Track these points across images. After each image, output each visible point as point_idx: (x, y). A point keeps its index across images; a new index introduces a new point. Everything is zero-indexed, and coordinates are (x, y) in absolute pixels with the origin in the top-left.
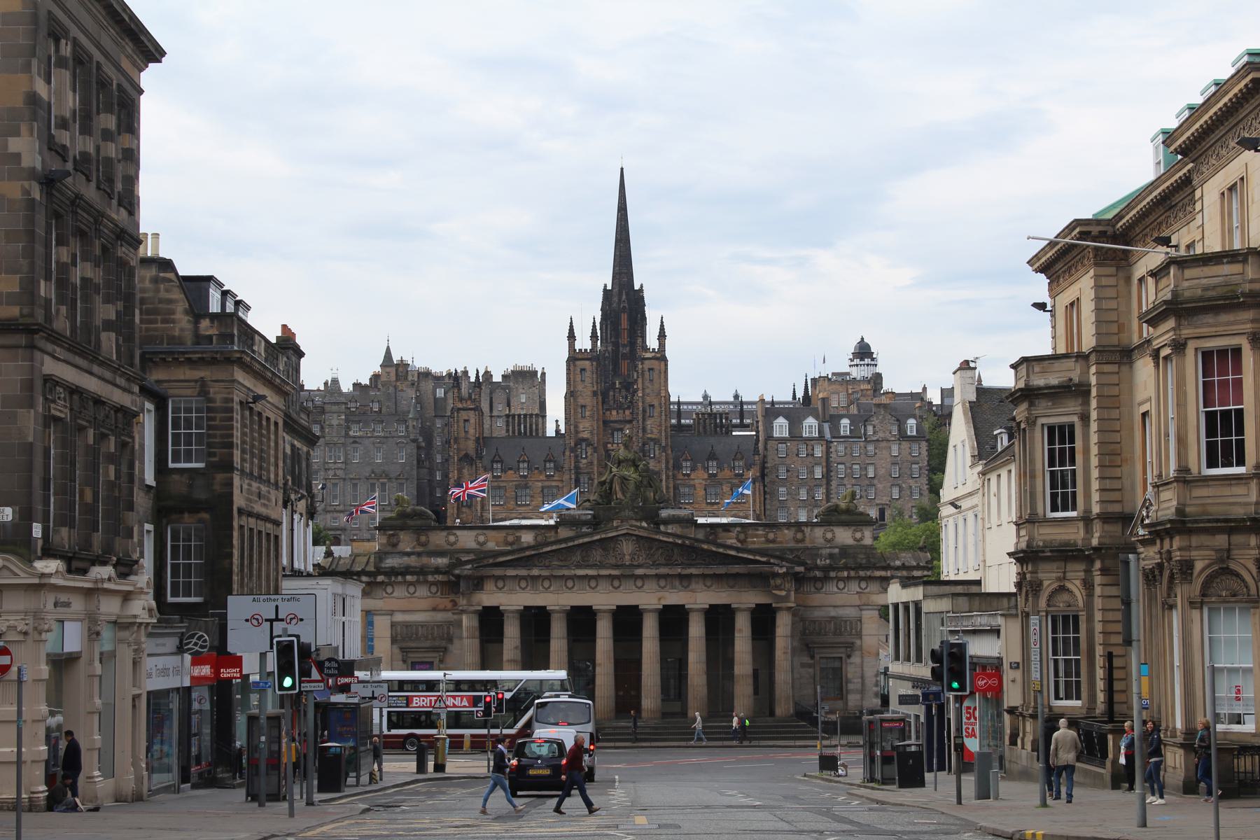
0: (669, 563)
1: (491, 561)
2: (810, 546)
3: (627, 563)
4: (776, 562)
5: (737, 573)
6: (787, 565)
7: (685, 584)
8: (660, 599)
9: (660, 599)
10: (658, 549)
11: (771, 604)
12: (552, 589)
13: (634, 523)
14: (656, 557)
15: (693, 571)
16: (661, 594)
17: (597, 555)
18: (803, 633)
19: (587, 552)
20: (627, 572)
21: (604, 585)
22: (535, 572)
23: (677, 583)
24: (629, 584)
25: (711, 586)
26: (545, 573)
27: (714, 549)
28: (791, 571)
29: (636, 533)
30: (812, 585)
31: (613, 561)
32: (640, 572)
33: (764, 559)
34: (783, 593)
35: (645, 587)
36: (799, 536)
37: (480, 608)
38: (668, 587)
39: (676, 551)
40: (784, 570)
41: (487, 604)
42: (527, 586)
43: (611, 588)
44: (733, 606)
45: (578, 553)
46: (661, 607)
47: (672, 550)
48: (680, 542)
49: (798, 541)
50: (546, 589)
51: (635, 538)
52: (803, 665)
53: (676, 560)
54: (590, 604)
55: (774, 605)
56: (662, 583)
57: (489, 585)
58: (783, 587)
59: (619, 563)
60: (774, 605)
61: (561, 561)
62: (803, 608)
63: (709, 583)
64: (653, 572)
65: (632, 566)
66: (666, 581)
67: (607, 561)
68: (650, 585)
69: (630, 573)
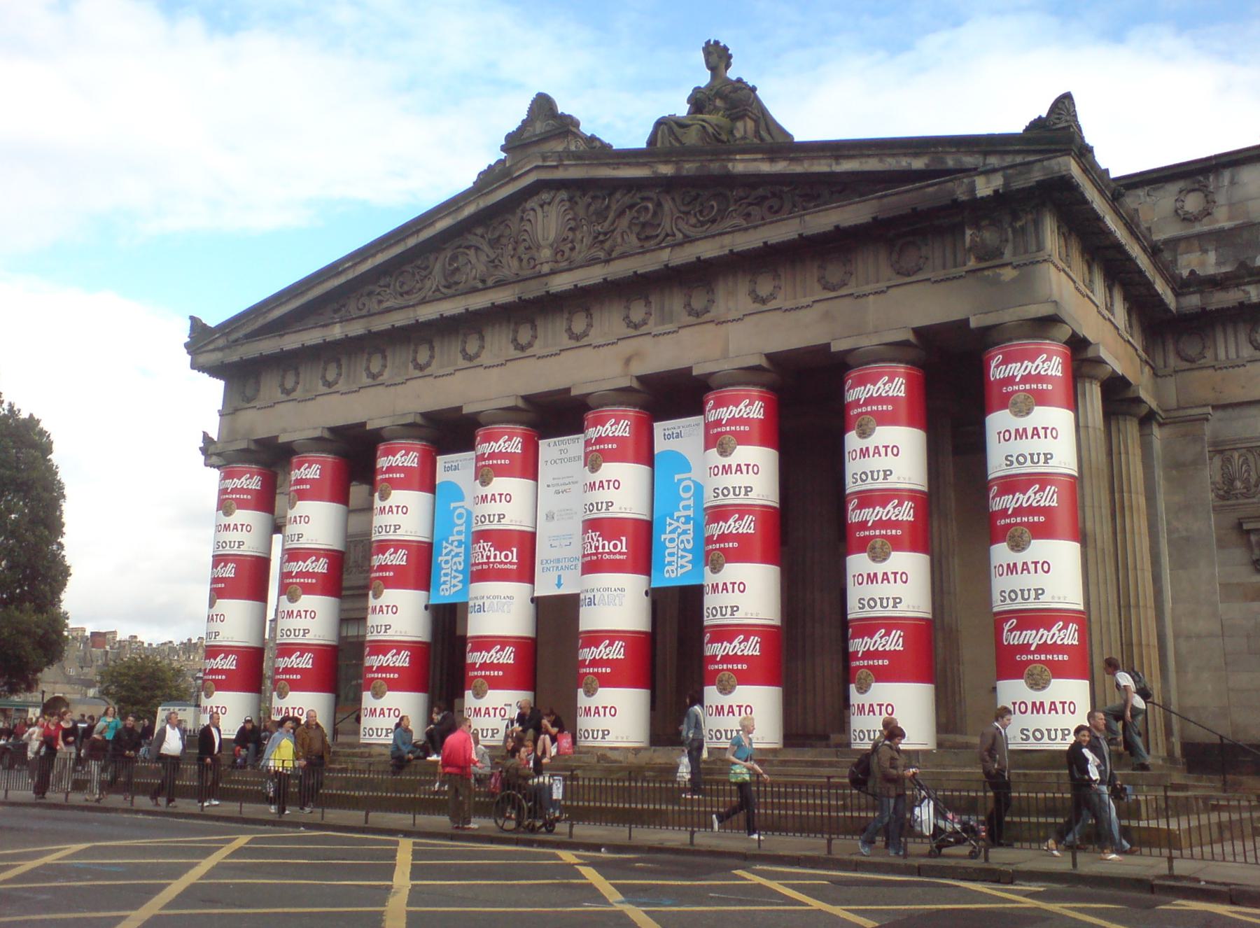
0: (648, 236)
1: (261, 322)
2: (1227, 225)
3: (546, 269)
4: (969, 161)
5: (837, 227)
6: (1009, 160)
7: (697, 303)
8: (628, 361)
9: (628, 361)
10: (621, 214)
11: (967, 321)
12: (386, 375)
13: (559, 146)
14: (617, 234)
15: (708, 249)
16: (626, 347)
17: (476, 264)
18: (1226, 492)
19: (454, 258)
20: (533, 290)
21: (497, 343)
22: (337, 332)
23: (676, 302)
24: (553, 333)
25: (772, 296)
26: (356, 329)
27: (765, 168)
28: (1019, 184)
29: (560, 174)
30: (1243, 337)
31: (511, 267)
32: (562, 283)
33: (918, 164)
34: (1008, 274)
35: (592, 332)
36: (1193, 203)
37: (243, 445)
38: (652, 321)
39: (668, 205)
40: (997, 182)
41: (262, 433)
42: (340, 375)
43: (513, 353)
44: (836, 347)
45: (438, 268)
46: (624, 383)
47: (659, 205)
48: (666, 170)
49: (1188, 219)
50: (374, 377)
51: (563, 195)
52: (1230, 591)
53: (667, 235)
54: (457, 404)
55: (973, 324)
56: (637, 313)
57: (270, 387)
58: (1008, 256)
59: (527, 273)
60: (973, 324)
61: (402, 295)
62: (1219, 414)
63: (764, 288)
64: (593, 275)
65: (553, 272)
66: (648, 303)
67: (499, 274)
68: (609, 322)
69: (541, 292)
